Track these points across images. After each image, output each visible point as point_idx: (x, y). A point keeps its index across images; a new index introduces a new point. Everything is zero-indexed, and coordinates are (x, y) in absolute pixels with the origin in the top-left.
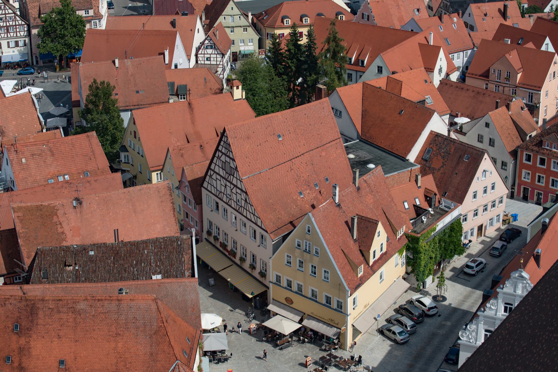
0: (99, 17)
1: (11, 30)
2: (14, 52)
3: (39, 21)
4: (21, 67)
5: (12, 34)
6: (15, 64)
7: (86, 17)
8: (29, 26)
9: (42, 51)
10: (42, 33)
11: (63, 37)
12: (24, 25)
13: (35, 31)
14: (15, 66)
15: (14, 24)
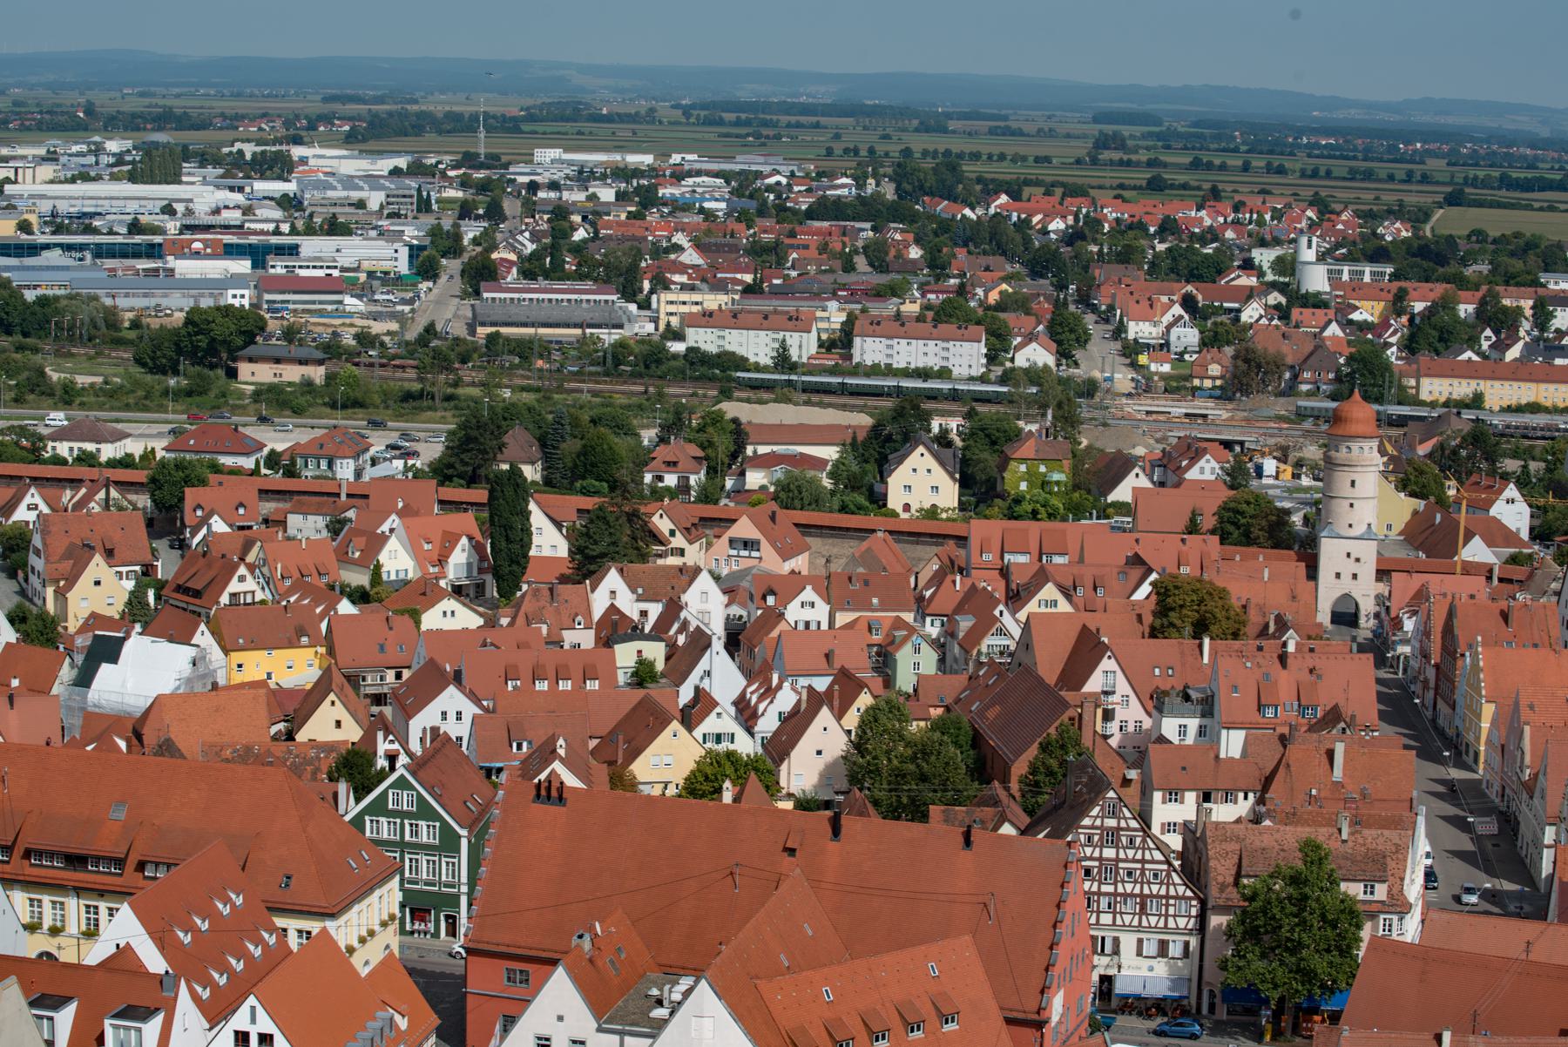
0: (1400, 906)
1: (1152, 907)
2: (1151, 969)
3: (1233, 894)
4: (1165, 1014)
5: (1153, 920)
6: (1149, 1003)
7: (1364, 902)
8: (1203, 903)
9: (1233, 980)
10: (1239, 930)
11: (1296, 948)
12: (1190, 898)
13: (1217, 921)
14: (1148, 1009)
15: (1163, 892)
